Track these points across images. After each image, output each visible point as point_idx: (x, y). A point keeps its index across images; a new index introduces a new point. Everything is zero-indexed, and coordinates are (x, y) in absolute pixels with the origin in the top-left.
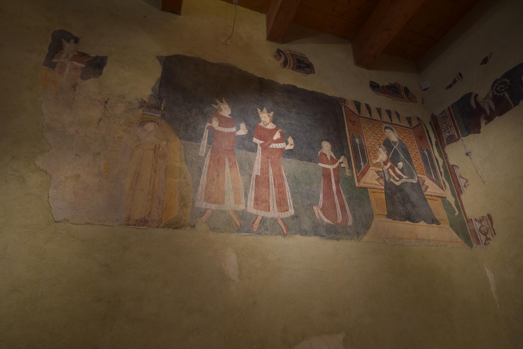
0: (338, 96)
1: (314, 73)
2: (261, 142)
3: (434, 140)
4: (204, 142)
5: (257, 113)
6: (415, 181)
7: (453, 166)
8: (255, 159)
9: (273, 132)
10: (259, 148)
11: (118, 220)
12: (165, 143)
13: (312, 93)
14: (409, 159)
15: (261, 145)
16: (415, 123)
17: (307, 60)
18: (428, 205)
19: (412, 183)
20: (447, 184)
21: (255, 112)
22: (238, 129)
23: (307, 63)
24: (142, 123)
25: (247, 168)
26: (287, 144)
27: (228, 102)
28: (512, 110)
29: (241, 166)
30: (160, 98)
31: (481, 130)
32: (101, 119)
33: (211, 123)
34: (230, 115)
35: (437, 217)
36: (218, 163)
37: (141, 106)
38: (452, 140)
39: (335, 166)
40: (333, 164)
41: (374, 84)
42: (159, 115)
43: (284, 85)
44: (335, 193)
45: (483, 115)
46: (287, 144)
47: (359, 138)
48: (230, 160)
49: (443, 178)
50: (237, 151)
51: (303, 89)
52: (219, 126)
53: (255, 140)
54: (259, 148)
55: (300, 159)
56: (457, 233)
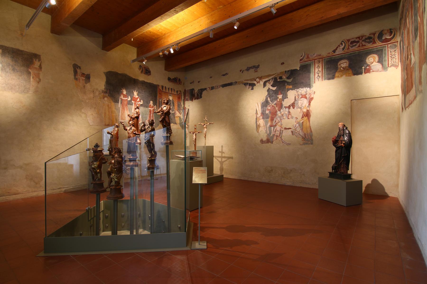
0: (157, 84)
1: (151, 75)
2: (134, 102)
3: (183, 98)
4: (120, 103)
5: (133, 92)
6: (173, 112)
7: (186, 107)
8: (132, 107)
9: (138, 98)
10: (134, 104)
11: (103, 125)
12: (110, 104)
13: (150, 83)
14: (174, 105)
15: (134, 103)
16: (179, 93)
17: (149, 69)
18: (175, 119)
19: (172, 113)
20: (182, 113)
21: (132, 92)
22: (128, 98)
23: (149, 71)
24: (104, 98)
25: (131, 110)
26: (141, 102)
27: (125, 89)
28: (198, 100)
29: (129, 110)
30: (107, 89)
31: (193, 101)
32: (93, 97)
33: (121, 96)
34: (126, 94)
35: (176, 122)
36: (124, 109)
37: (103, 92)
38: (187, 100)
39: (153, 109)
40: (153, 108)
41: (169, 78)
42: (107, 95)
43: (141, 81)
44: (152, 116)
45: (194, 97)
46: (141, 102)
47: (161, 99)
48: (126, 108)
49: (181, 111)
50: (128, 105)
51: (147, 82)
52: (123, 97)
53: (133, 102)
54: (134, 104)
55: (144, 107)
56: (181, 126)
